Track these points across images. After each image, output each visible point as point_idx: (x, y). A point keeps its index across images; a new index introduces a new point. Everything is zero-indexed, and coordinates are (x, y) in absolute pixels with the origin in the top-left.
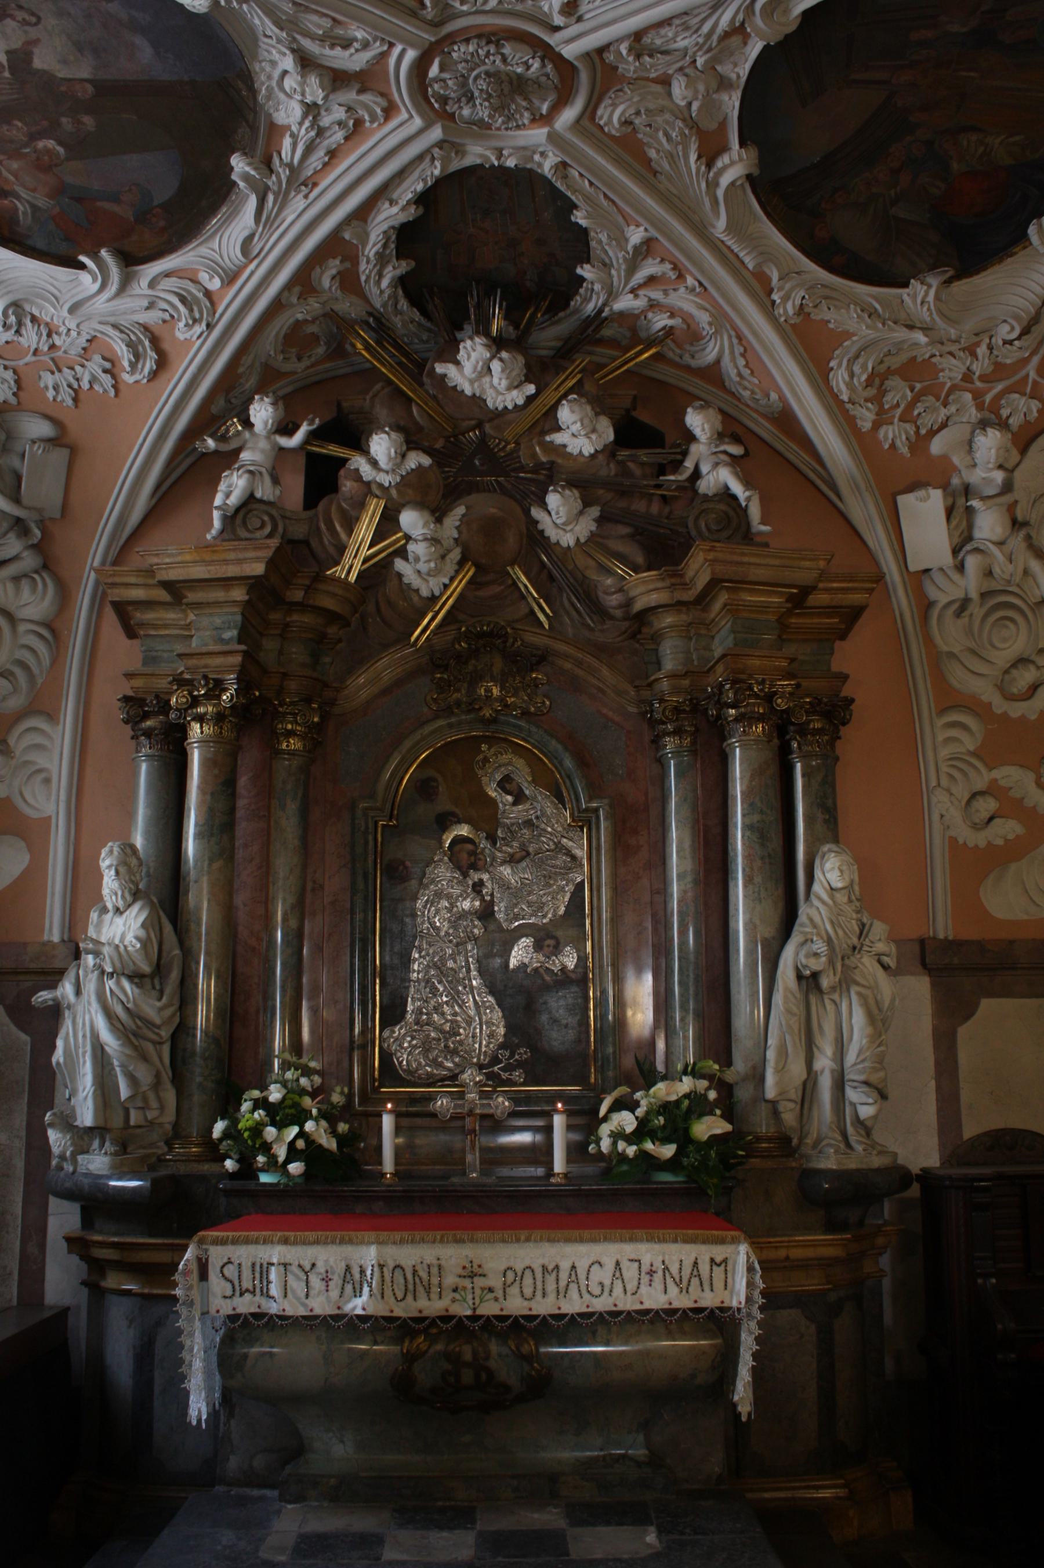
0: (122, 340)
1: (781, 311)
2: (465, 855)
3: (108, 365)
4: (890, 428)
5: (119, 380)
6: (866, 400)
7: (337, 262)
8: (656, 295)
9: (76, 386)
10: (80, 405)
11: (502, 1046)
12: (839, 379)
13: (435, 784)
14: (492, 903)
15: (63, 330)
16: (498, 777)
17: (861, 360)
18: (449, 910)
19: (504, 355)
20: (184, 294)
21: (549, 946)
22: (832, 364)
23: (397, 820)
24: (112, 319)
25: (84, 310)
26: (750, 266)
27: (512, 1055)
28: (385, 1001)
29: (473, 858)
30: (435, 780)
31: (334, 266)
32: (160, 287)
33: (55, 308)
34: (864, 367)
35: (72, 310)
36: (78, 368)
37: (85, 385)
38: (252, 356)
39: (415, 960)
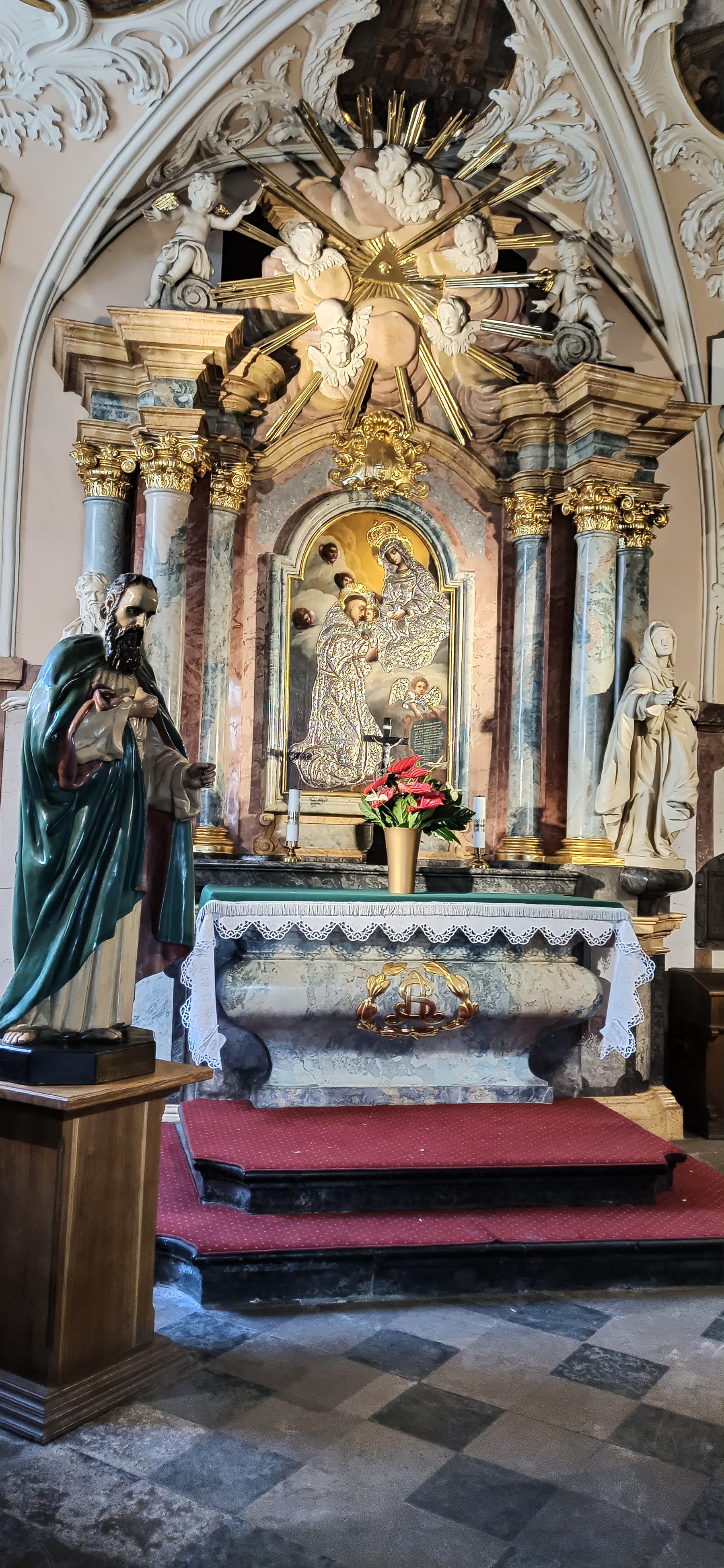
0: (78, 95)
1: (659, 159)
3: (58, 118)
4: (719, 277)
5: (67, 135)
6: (706, 251)
7: (291, 50)
8: (554, 130)
9: (23, 134)
10: (24, 153)
12: (689, 230)
15: (17, 71)
17: (711, 214)
19: (419, 167)
20: (145, 57)
22: (687, 215)
24: (70, 71)
25: (41, 57)
26: (646, 114)
31: (286, 53)
32: (121, 45)
33: (15, 48)
34: (712, 220)
35: (31, 52)
36: (28, 116)
37: (33, 134)
38: (193, 133)
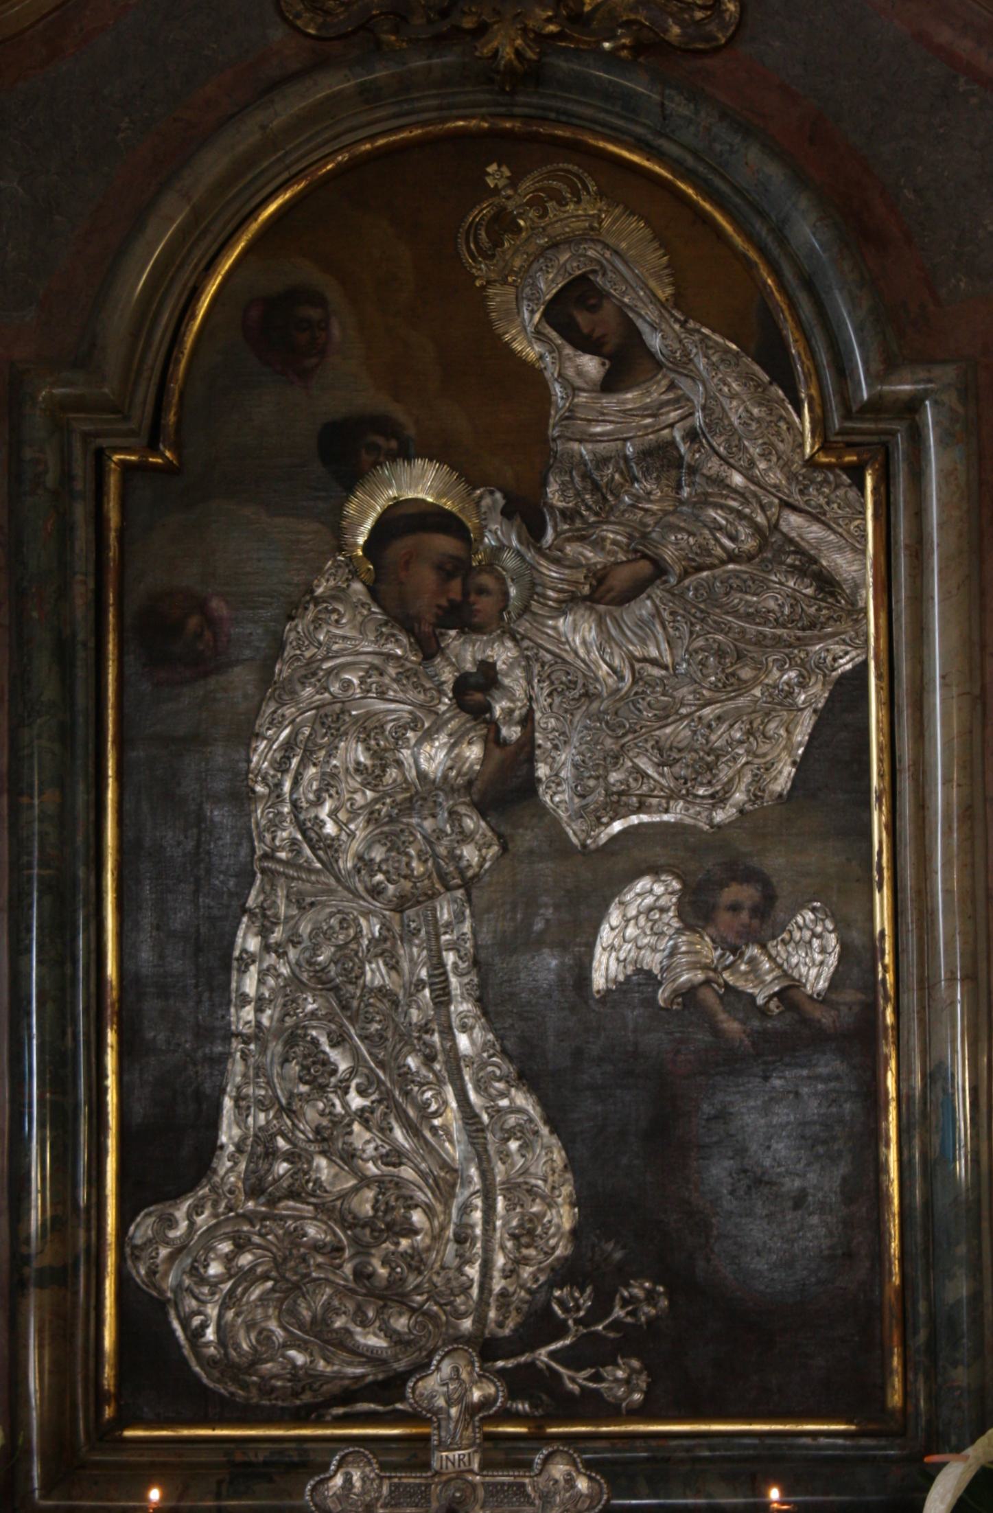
2: (426, 577)
11: (565, 1273)
13: (314, 313)
14: (526, 751)
16: (548, 285)
18: (371, 776)
21: (735, 908)
23: (177, 448)
27: (601, 1308)
28: (139, 1110)
29: (456, 586)
30: (319, 300)
39: (247, 960)
